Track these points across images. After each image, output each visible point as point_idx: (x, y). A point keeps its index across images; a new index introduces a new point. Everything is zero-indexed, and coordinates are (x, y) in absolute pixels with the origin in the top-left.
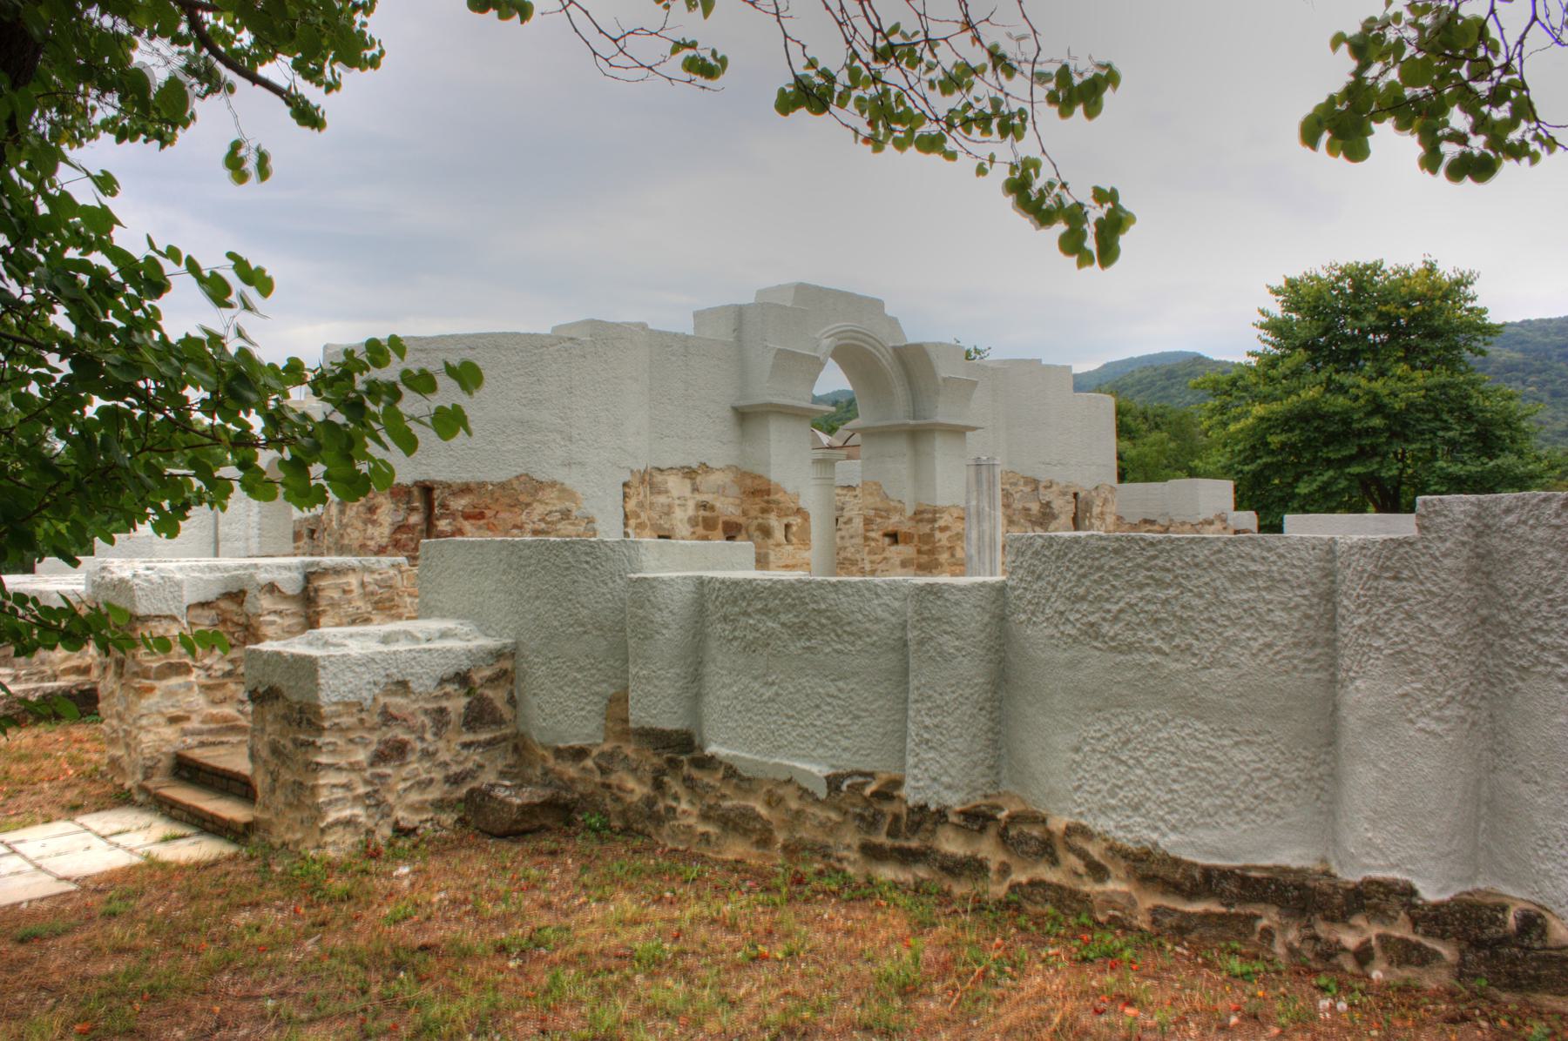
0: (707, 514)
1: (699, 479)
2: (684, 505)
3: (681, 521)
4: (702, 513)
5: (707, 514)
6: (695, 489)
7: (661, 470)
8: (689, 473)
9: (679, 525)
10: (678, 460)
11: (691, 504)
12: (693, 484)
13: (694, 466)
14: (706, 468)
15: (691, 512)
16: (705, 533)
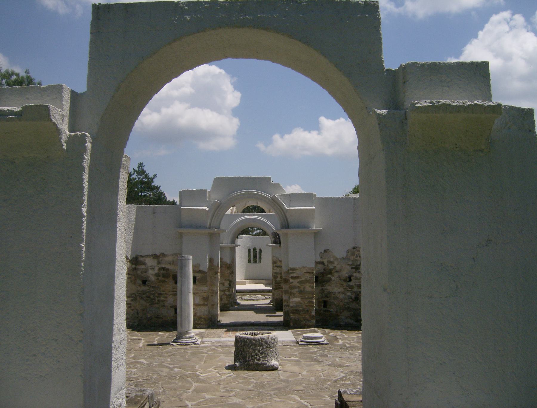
0: (165, 272)
1: (161, 259)
2: (153, 269)
3: (152, 275)
4: (162, 271)
5: (165, 272)
6: (159, 263)
7: (143, 256)
8: (155, 256)
9: (151, 276)
10: (150, 253)
11: (157, 269)
12: (158, 261)
13: (158, 254)
14: (163, 255)
15: (156, 271)
16: (163, 279)
